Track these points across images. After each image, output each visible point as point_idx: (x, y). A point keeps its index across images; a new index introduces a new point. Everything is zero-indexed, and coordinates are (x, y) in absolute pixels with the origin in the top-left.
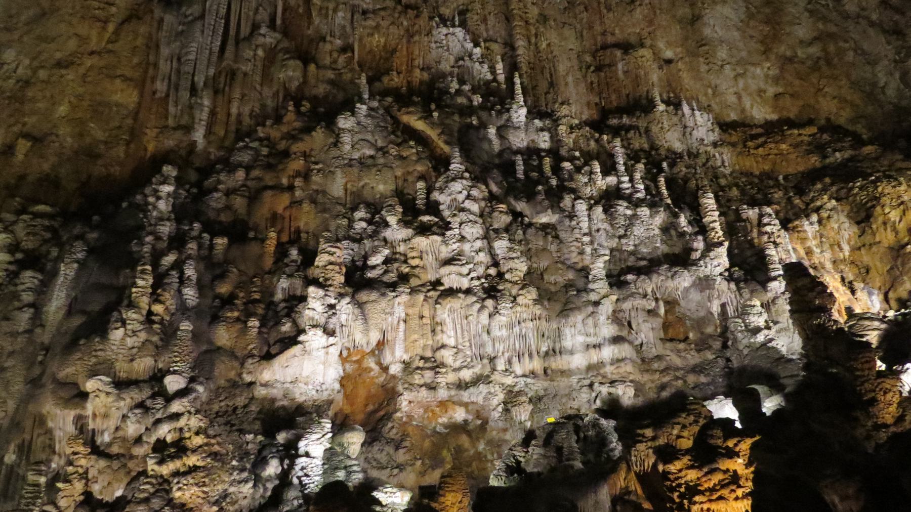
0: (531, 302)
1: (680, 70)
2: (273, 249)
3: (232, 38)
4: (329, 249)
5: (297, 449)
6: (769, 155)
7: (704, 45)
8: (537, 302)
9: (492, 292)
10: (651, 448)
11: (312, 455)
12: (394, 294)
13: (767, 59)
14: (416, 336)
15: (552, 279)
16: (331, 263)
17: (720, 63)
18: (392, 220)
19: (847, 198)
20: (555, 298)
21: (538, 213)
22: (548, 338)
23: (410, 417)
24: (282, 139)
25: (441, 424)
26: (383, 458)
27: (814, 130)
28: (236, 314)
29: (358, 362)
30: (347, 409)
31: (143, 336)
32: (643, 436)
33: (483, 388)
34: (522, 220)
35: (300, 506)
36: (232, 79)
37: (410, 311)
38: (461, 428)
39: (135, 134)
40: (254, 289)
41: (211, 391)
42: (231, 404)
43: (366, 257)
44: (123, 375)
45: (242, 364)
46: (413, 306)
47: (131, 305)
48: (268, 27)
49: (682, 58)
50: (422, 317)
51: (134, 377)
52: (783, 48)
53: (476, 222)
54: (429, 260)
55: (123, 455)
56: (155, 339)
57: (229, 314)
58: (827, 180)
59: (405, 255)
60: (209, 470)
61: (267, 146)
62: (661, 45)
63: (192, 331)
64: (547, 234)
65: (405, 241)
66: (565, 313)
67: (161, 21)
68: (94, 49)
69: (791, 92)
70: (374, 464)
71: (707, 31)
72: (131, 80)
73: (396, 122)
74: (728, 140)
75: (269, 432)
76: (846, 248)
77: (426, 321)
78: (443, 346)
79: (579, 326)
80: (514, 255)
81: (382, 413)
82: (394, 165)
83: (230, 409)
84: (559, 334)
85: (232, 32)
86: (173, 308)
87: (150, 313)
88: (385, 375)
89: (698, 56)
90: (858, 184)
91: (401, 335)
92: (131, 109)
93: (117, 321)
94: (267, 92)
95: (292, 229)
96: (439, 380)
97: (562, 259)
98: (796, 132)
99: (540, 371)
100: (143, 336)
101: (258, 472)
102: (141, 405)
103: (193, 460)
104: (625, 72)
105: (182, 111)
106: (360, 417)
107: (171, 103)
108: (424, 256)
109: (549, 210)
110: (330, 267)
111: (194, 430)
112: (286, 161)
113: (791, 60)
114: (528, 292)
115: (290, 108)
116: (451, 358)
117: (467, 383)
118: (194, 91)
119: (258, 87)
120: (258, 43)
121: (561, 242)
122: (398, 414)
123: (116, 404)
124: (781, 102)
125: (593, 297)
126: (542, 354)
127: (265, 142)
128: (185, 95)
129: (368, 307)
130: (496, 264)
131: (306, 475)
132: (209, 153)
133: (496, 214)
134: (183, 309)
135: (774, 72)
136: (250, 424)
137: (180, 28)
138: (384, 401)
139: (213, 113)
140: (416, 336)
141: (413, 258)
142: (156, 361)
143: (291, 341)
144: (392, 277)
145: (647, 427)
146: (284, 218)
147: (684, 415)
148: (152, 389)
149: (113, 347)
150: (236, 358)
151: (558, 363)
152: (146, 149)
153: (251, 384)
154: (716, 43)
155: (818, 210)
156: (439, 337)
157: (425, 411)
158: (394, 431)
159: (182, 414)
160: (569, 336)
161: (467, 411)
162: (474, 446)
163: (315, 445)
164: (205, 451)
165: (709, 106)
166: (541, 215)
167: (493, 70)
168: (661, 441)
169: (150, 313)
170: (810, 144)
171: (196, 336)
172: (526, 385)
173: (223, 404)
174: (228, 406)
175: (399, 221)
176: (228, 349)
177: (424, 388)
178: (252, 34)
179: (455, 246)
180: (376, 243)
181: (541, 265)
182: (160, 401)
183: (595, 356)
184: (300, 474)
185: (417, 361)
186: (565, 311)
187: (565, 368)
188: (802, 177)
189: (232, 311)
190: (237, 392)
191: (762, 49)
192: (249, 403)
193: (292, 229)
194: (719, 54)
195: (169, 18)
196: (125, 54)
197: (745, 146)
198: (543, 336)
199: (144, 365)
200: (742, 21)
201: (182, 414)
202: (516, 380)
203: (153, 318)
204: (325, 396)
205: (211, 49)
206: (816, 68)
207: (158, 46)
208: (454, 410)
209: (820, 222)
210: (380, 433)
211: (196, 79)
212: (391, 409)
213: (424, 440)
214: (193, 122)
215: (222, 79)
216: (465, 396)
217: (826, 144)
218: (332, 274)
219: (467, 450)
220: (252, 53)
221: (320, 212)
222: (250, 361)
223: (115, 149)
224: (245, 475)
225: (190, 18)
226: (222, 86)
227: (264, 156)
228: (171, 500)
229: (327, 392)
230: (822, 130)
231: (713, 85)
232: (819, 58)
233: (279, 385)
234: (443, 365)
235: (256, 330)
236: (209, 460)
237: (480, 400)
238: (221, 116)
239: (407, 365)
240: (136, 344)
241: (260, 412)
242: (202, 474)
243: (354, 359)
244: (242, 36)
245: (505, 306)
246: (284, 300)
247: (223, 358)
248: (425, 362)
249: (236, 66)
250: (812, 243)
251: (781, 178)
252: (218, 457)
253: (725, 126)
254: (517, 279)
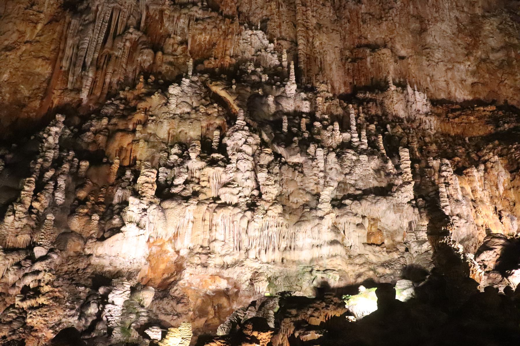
0: (277, 215)
1: (409, 64)
2: (116, 170)
4: (147, 173)
5: (108, 299)
6: (461, 123)
7: (427, 48)
8: (281, 215)
9: (252, 206)
10: (293, 321)
11: (115, 304)
12: (186, 204)
13: (468, 60)
14: (199, 232)
15: (295, 200)
16: (147, 182)
17: (436, 61)
18: (193, 155)
19: (507, 155)
20: (295, 213)
21: (291, 156)
22: (287, 238)
23: (191, 284)
24: (134, 99)
25: (210, 290)
26: (168, 308)
27: (493, 108)
28: (86, 211)
29: (161, 246)
30: (151, 276)
31: (25, 221)
32: (290, 313)
33: (238, 269)
34: (281, 159)
35: (105, 334)
36: (109, 60)
37: (197, 216)
38: (225, 293)
39: (47, 93)
40: (101, 195)
41: (63, 258)
42: (75, 267)
43: (173, 179)
44: (10, 244)
45: (85, 243)
46: (199, 213)
47: (21, 202)
48: (134, 28)
49: (411, 56)
50: (204, 220)
51: (17, 246)
52: (480, 53)
53: (248, 160)
54: (214, 183)
55: (4, 294)
56: (32, 223)
57: (81, 211)
58: (497, 142)
59: (199, 179)
60: (50, 307)
61: (123, 104)
62: (398, 46)
63: (54, 220)
64: (295, 169)
65: (200, 169)
66: (299, 223)
67: (70, 23)
69: (482, 82)
70: (163, 311)
71: (429, 40)
72: (48, 59)
73: (209, 90)
74: (436, 112)
75: (95, 287)
76: (501, 189)
77: (207, 223)
78: (215, 240)
79: (309, 232)
80: (269, 183)
81: (172, 280)
82: (201, 119)
83: (74, 270)
84: (293, 237)
85: (112, 31)
86: (46, 205)
87: (31, 207)
88: (177, 256)
89: (422, 55)
90: (515, 146)
91: (189, 230)
92: (46, 77)
93: (10, 211)
94: (130, 69)
95: (132, 158)
96: (209, 262)
97: (303, 187)
98: (482, 108)
99: (279, 260)
100: (25, 221)
101: (83, 310)
102: (19, 264)
103: (42, 300)
104: (372, 64)
105: (76, 79)
106: (158, 281)
107: (70, 74)
108: (211, 180)
109: (299, 154)
110: (146, 185)
111: (46, 282)
112: (133, 113)
113: (484, 60)
114: (276, 208)
115: (141, 80)
116: (220, 248)
117: (228, 265)
118: (84, 67)
119: (124, 66)
120: (127, 38)
121: (304, 175)
122: (182, 282)
123: (3, 262)
124: (475, 89)
125: (320, 213)
126: (282, 248)
127: (123, 101)
128: (79, 70)
129: (168, 212)
130: (258, 188)
131: (111, 316)
132: (90, 107)
133: (263, 155)
134: (53, 205)
135: (473, 68)
136: (85, 280)
137: (81, 28)
138: (174, 272)
139: (94, 82)
140: (199, 232)
141: (204, 181)
142: (31, 237)
143: (117, 230)
144: (188, 193)
145: (294, 308)
146: (127, 150)
147: (318, 302)
148: (27, 254)
149: (6, 227)
150: (82, 238)
151: (290, 256)
152: (53, 103)
153: (90, 255)
154: (435, 47)
155: (485, 162)
156: (213, 234)
157: (201, 281)
158: (177, 292)
159: (41, 271)
160: (301, 238)
161: (228, 283)
162: (230, 305)
163: (118, 298)
164: (49, 296)
165: (427, 88)
166: (293, 157)
167: (280, 58)
168: (299, 318)
169: (31, 207)
170: (490, 117)
171: (57, 223)
172: (268, 268)
173: (70, 266)
174: (74, 268)
175: (198, 156)
176: (78, 232)
177: (199, 266)
178: (124, 32)
179: (232, 175)
180: (182, 170)
181: (289, 191)
182: (29, 262)
183: (316, 253)
184: (108, 314)
185: (198, 249)
186: (300, 222)
187: (296, 259)
188: (482, 139)
189: (83, 208)
190: (80, 260)
191: (466, 53)
192: (87, 267)
193: (132, 158)
194: (436, 54)
195: (74, 22)
196: (46, 43)
197: (447, 116)
198: (284, 237)
199: (23, 239)
200: (454, 34)
201: (41, 271)
202: (261, 265)
203: (33, 210)
204: (135, 266)
205: (97, 41)
206: (501, 67)
207: (66, 39)
208: (220, 281)
209: (486, 170)
210: (169, 292)
211: (86, 60)
212: (178, 277)
213: (197, 299)
214: (82, 87)
215: (103, 61)
216: (226, 273)
217: (500, 118)
218: (146, 189)
219: (225, 308)
220: (122, 44)
221: (151, 148)
222: (90, 241)
223: (34, 102)
224: (73, 312)
225: (87, 22)
226: (102, 64)
227: (121, 110)
228: (25, 323)
229: (137, 264)
230: (499, 108)
231: (431, 75)
232: (503, 60)
233: (107, 257)
234: (213, 252)
235: (97, 222)
236: (51, 301)
237: (235, 277)
238: (99, 84)
239: (191, 250)
240: (20, 226)
241: (93, 274)
242: (45, 310)
243: (158, 244)
244: (118, 34)
245: (259, 215)
246: (118, 204)
247: (74, 238)
248: (203, 250)
249: (111, 52)
250: (477, 185)
251: (467, 139)
252: (58, 300)
253: (434, 102)
254: (270, 199)
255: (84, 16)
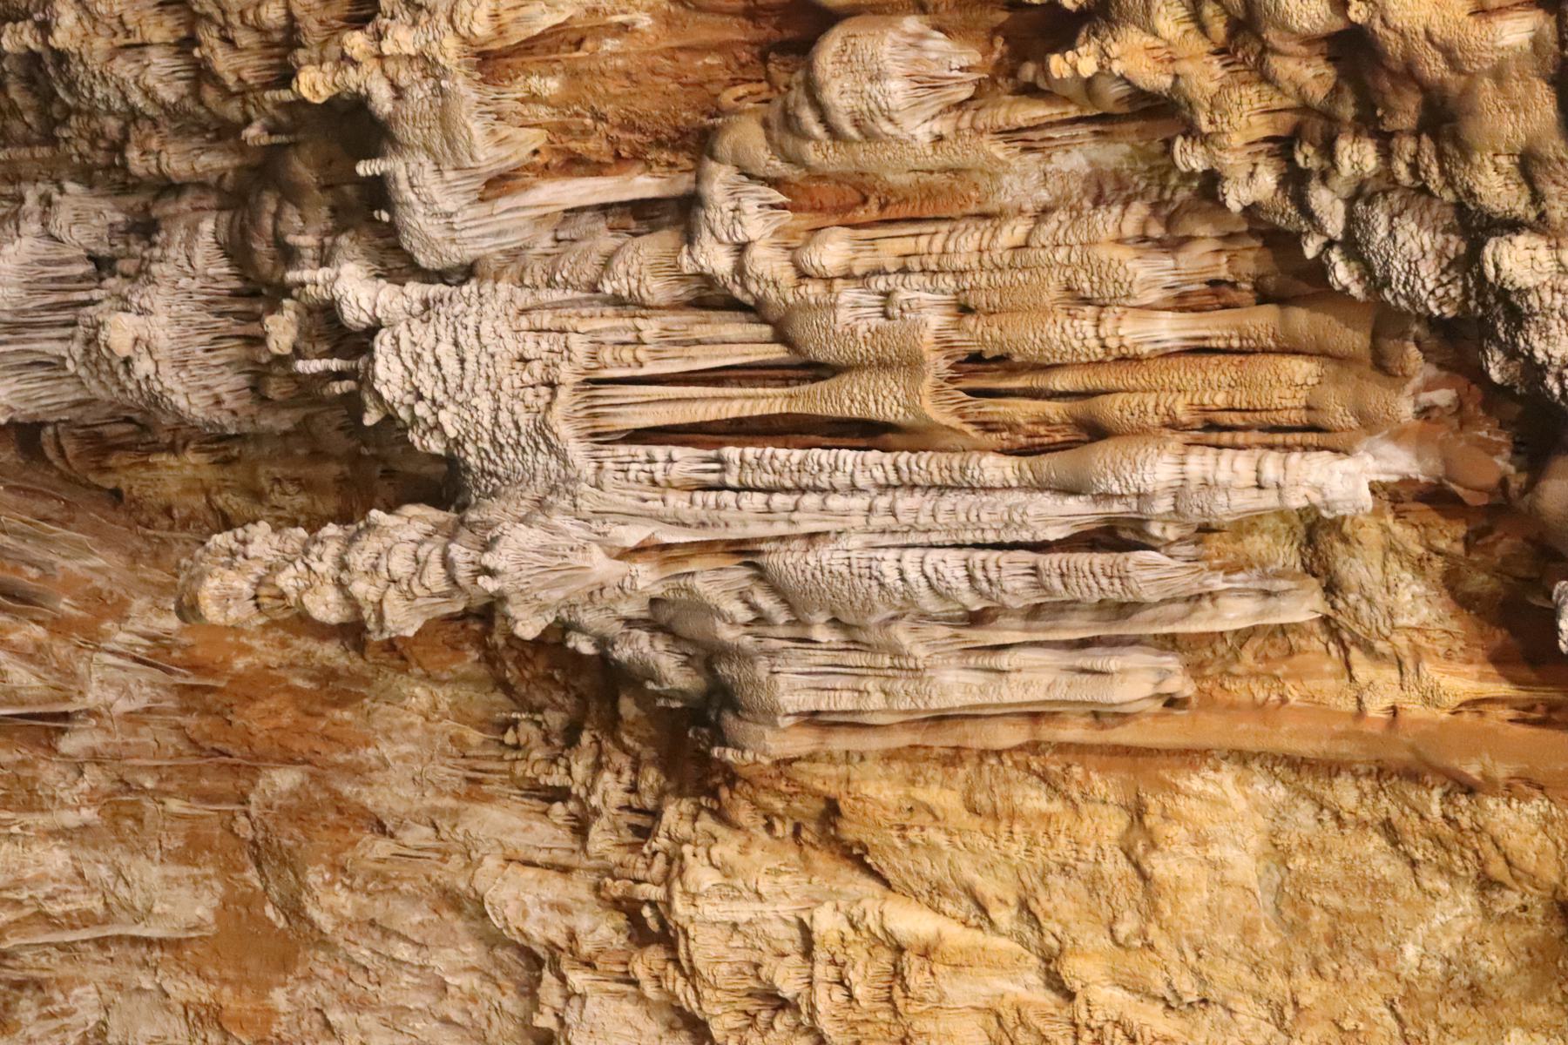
3: (800, 400)
24: (1265, 78)
36: (1003, 362)
39: (1402, 766)
48: (690, 238)
61: (1328, 149)
67: (812, 719)
68: (1035, 979)
72: (1138, 813)
85: (769, 401)
92: (1279, 792)
94: (1021, 181)
105: (1230, 569)
107: (1198, 625)
112: (1393, 46)
115: (1088, 67)
118: (1113, 537)
119: (1015, 231)
120: (787, 275)
127: (1305, 156)
128: (1146, 573)
132: (1425, 412)
137: (822, 634)
139: (1211, 429)
152: (1477, 704)
178: (754, 310)
195: (793, 687)
196: (1017, 850)
205: (885, 488)
207: (940, 719)
211: (1052, 534)
214: (1282, 514)
215: (1021, 410)
220: (848, 294)
223: (1514, 842)
225: (766, 602)
226: (1053, 409)
227: (1386, 153)
238: (1215, 387)
244: (777, 353)
249: (937, 364)
255: (727, 634)
